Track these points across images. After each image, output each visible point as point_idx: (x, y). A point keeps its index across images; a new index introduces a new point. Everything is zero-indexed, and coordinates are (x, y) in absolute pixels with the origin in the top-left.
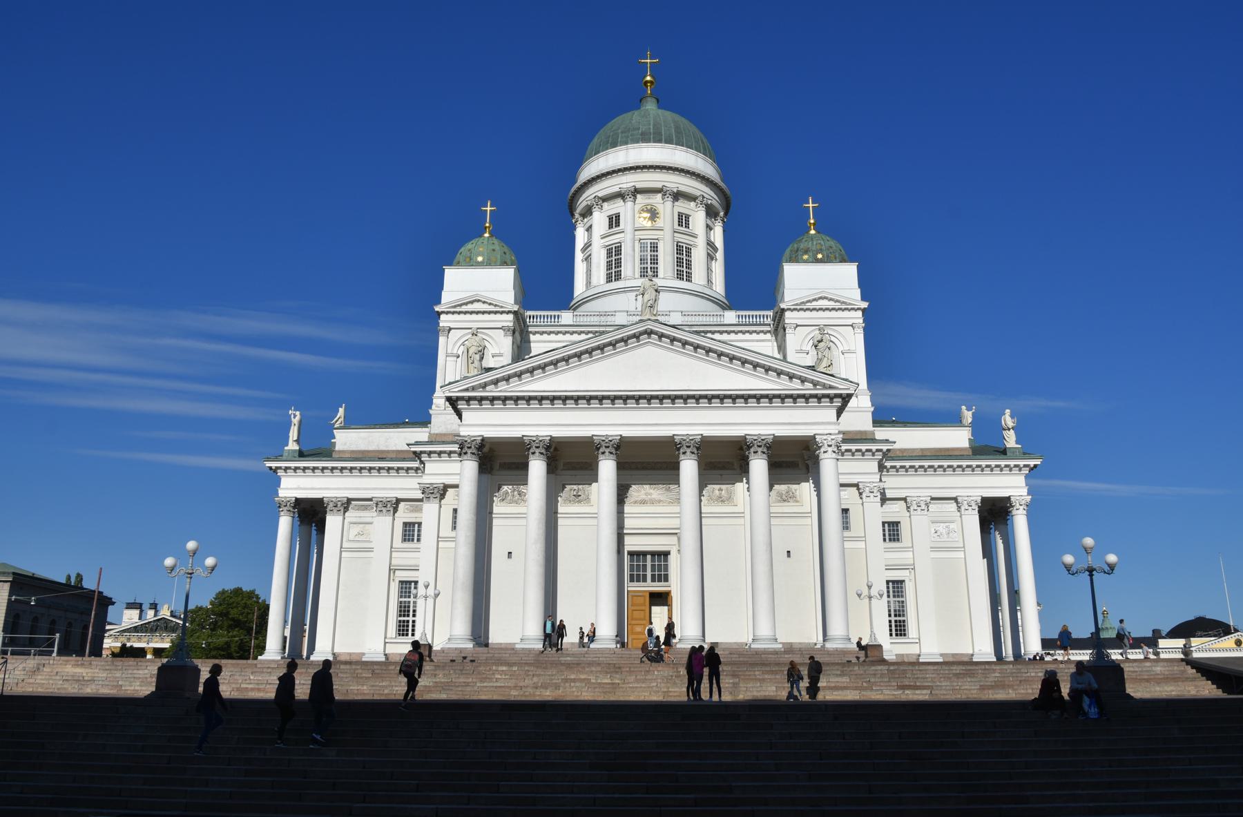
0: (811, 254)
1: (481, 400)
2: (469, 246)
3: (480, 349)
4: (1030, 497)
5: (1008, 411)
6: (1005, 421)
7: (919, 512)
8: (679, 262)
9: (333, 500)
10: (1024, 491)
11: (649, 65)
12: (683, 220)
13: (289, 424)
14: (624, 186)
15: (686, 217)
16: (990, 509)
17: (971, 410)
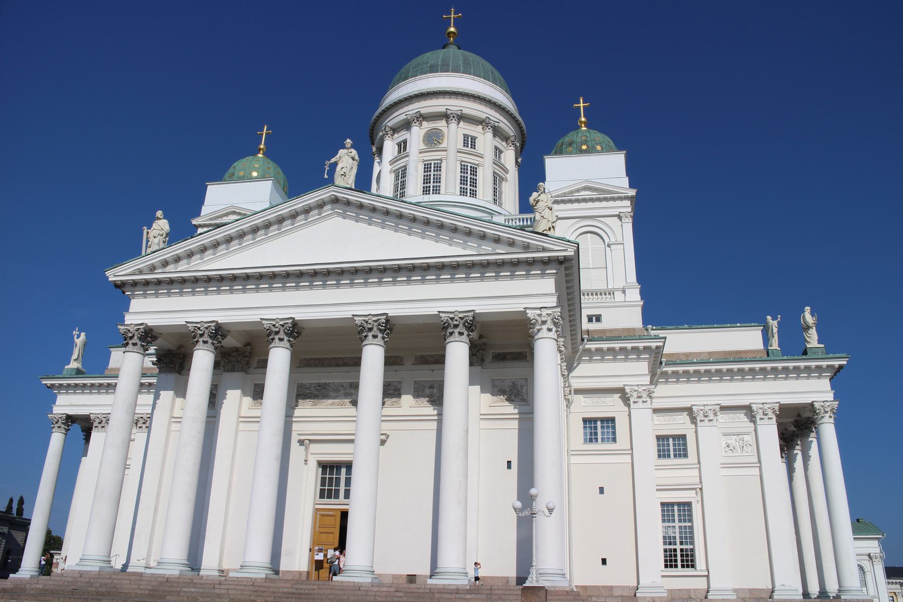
0: (575, 146)
1: (147, 283)
2: (234, 165)
3: (161, 233)
4: (837, 403)
5: (808, 309)
6: (804, 317)
7: (706, 423)
8: (463, 181)
9: (99, 416)
10: (830, 396)
11: (452, 21)
12: (470, 141)
13: (72, 344)
14: (410, 113)
15: (471, 139)
16: (796, 421)
17: (777, 320)
